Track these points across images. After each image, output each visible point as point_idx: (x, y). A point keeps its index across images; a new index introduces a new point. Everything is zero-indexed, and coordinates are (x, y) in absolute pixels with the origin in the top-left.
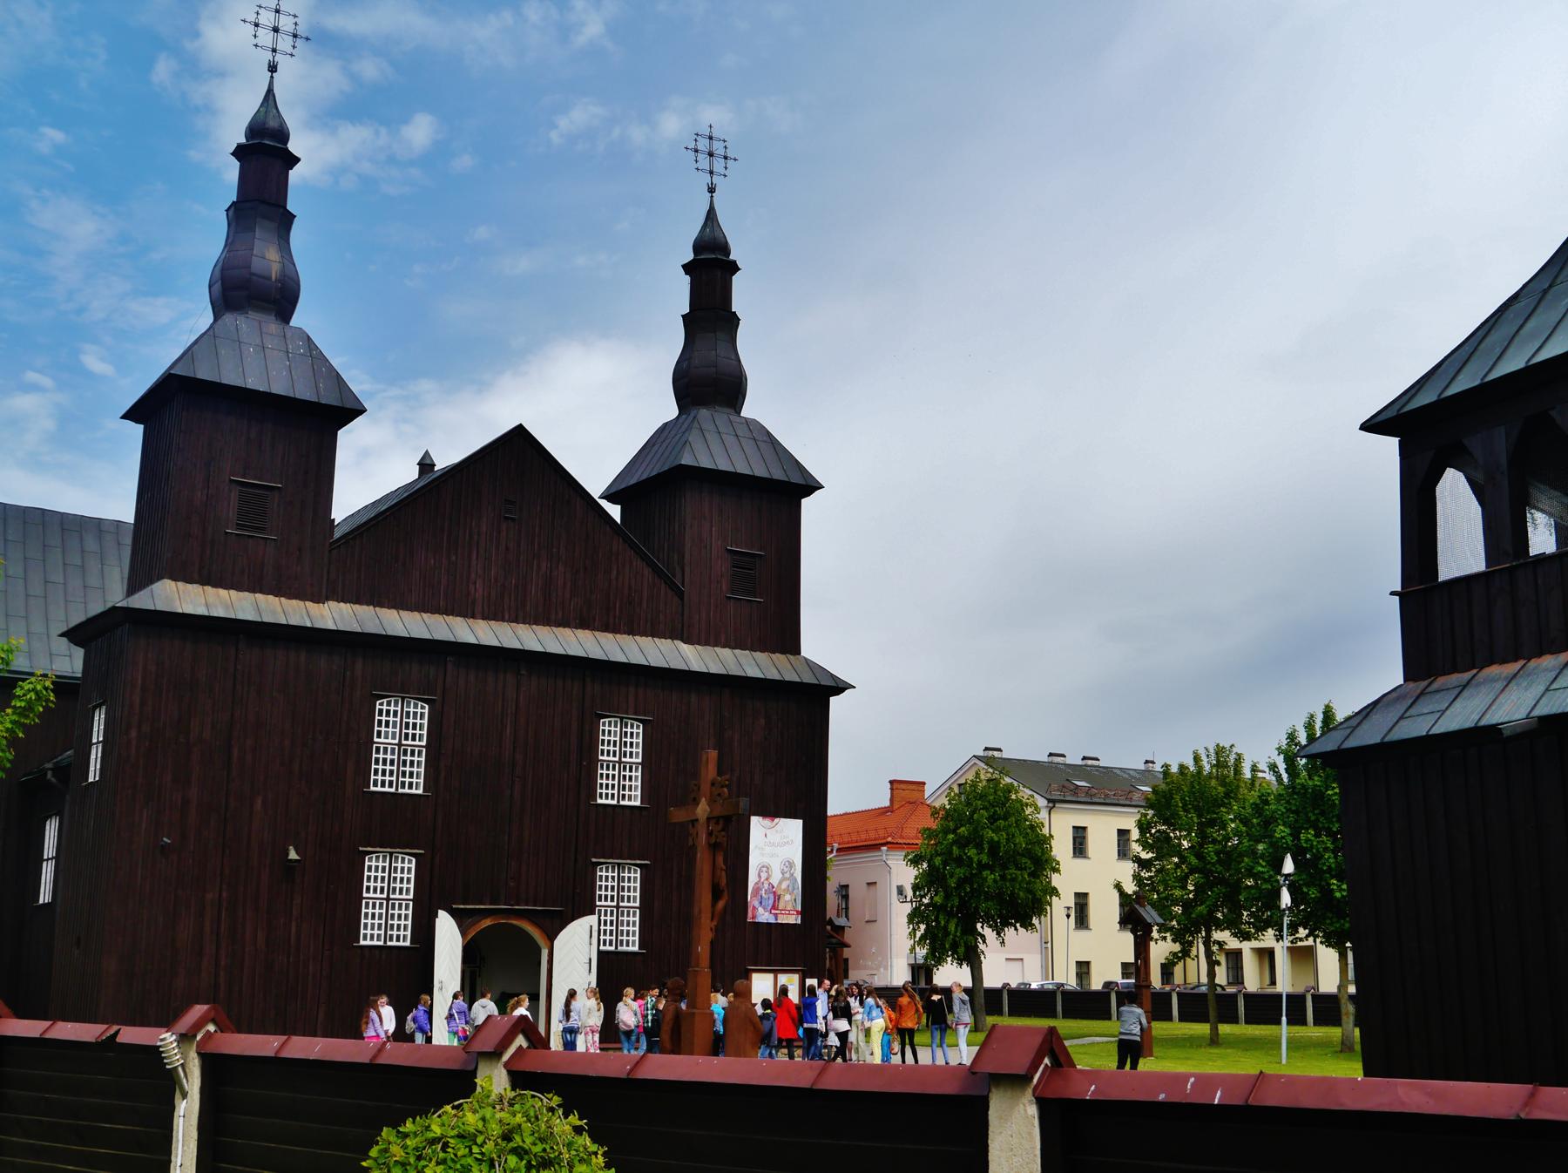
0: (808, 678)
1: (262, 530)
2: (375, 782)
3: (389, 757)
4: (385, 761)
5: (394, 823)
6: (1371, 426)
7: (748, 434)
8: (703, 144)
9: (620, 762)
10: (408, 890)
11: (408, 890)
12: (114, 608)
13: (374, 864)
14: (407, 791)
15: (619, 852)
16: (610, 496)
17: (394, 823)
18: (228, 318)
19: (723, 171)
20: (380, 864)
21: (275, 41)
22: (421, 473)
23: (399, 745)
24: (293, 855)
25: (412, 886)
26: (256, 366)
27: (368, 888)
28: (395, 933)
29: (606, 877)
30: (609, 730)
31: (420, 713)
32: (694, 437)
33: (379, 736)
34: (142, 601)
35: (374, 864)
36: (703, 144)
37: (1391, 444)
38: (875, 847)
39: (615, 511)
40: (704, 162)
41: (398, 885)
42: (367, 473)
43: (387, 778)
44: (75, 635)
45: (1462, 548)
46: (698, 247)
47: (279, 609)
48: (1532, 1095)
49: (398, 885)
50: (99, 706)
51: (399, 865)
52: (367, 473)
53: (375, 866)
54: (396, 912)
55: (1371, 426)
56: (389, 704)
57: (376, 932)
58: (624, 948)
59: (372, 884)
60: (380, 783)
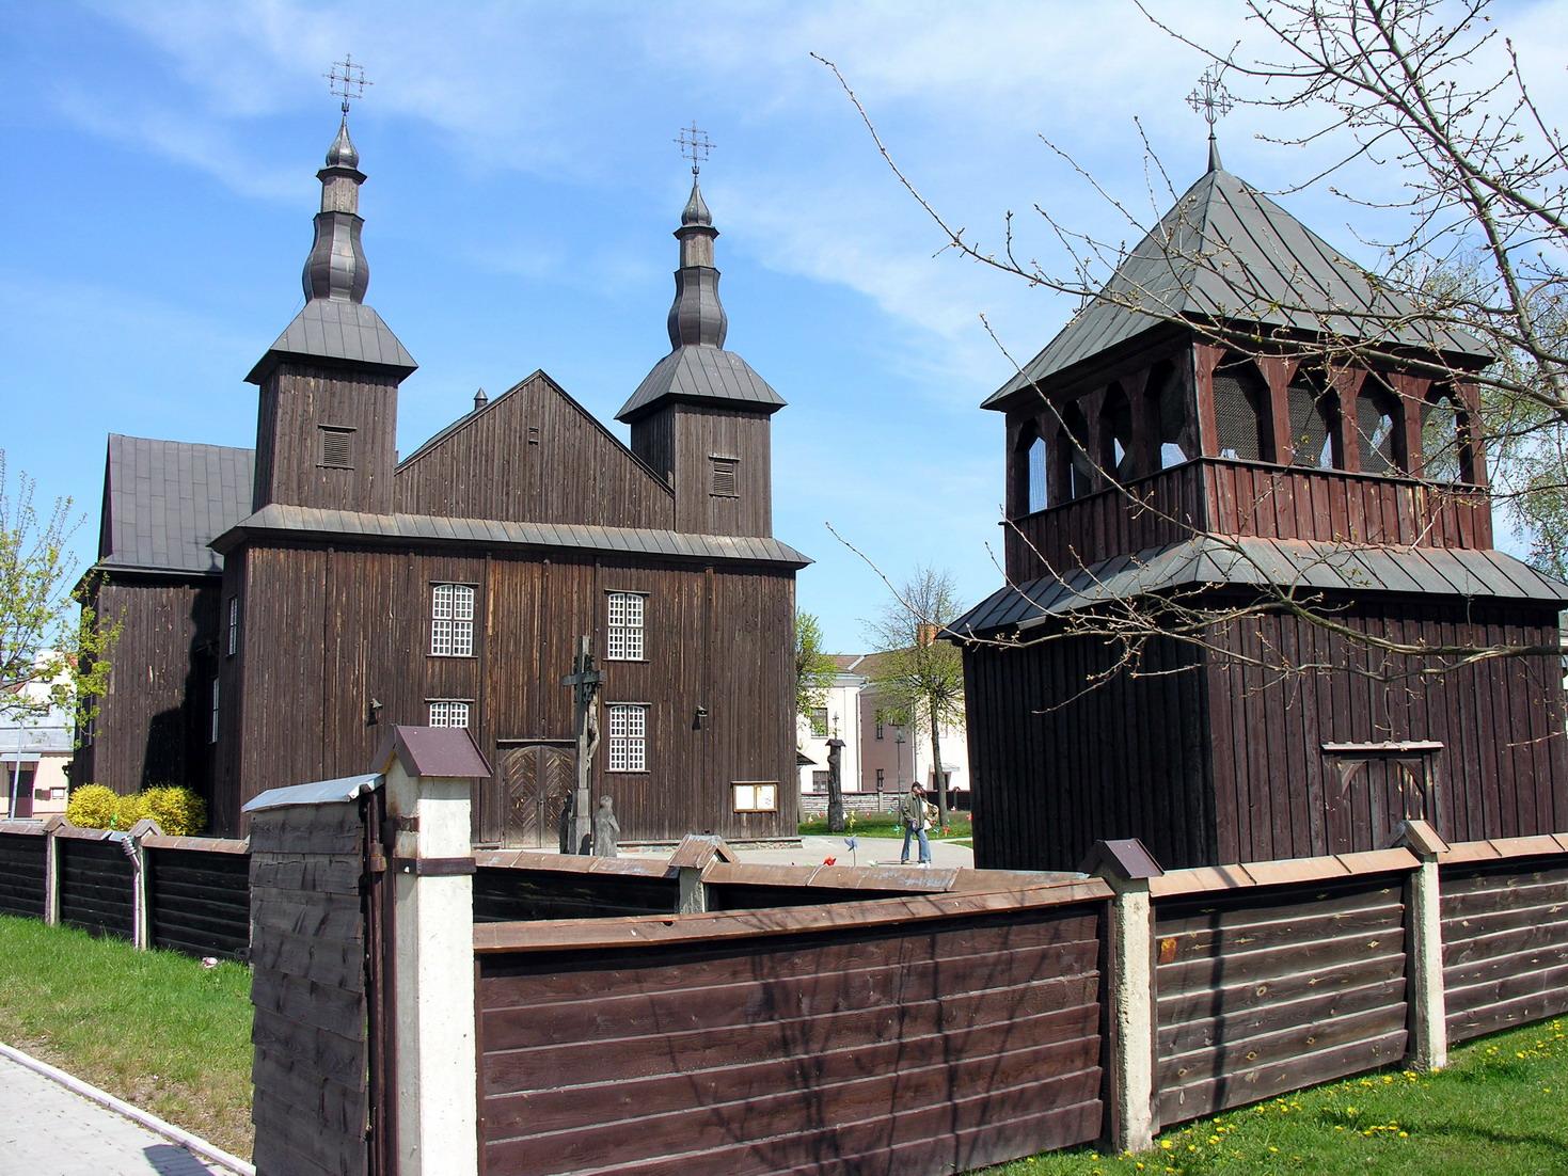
0: (777, 556)
1: (344, 461)
2: (435, 649)
3: (445, 630)
6: (988, 406)
7: (726, 364)
8: (688, 136)
9: (626, 627)
12: (236, 528)
13: (437, 710)
16: (623, 418)
18: (315, 302)
19: (705, 157)
20: (442, 710)
21: (347, 88)
22: (477, 406)
26: (335, 332)
30: (615, 604)
32: (682, 369)
33: (437, 615)
34: (257, 521)
35: (437, 710)
36: (688, 136)
37: (1000, 417)
39: (623, 432)
40: (689, 150)
42: (421, 415)
43: (444, 646)
44: (216, 545)
46: (685, 219)
47: (357, 522)
50: (233, 598)
51: (456, 711)
52: (421, 415)
55: (988, 406)
60: (440, 647)
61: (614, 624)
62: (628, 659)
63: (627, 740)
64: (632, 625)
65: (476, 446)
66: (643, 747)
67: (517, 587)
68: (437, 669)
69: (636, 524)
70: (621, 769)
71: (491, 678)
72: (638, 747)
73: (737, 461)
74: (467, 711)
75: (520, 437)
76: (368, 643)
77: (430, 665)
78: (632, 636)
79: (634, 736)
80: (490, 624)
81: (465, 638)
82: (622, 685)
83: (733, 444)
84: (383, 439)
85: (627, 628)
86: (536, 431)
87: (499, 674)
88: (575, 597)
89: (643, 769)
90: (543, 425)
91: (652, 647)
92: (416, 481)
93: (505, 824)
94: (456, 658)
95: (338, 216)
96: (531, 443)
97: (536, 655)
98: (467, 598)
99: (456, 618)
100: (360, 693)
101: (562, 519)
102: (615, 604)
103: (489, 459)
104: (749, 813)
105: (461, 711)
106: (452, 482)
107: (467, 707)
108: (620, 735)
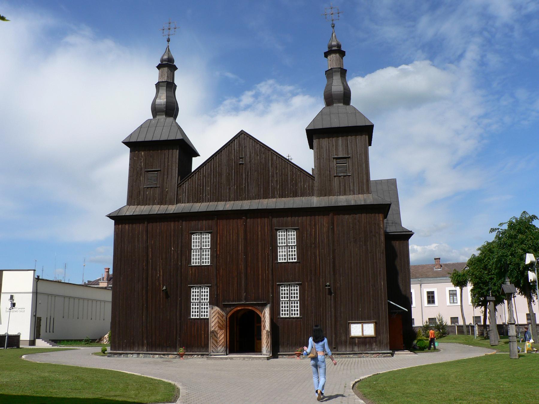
5: (201, 276)
10: (207, 299)
13: (194, 290)
14: (204, 264)
15: (289, 281)
17: (201, 276)
20: (197, 290)
23: (201, 249)
24: (164, 288)
25: (208, 297)
27: (193, 299)
28: (203, 314)
29: (284, 290)
31: (207, 238)
38: (85, 286)
41: (203, 297)
49: (203, 297)
51: (203, 290)
53: (195, 292)
54: (203, 306)
57: (196, 314)
59: (194, 297)
60: (195, 261)
64: (290, 244)
66: (298, 305)
68: (194, 272)
69: (295, 195)
70: (286, 316)
72: (296, 305)
73: (349, 158)
74: (208, 290)
78: (291, 250)
79: (293, 299)
81: (207, 257)
84: (172, 172)
85: (287, 246)
88: (260, 233)
89: (299, 316)
90: (246, 155)
95: (160, 83)
101: (258, 197)
103: (220, 174)
104: (359, 338)
105: (206, 290)
108: (286, 299)
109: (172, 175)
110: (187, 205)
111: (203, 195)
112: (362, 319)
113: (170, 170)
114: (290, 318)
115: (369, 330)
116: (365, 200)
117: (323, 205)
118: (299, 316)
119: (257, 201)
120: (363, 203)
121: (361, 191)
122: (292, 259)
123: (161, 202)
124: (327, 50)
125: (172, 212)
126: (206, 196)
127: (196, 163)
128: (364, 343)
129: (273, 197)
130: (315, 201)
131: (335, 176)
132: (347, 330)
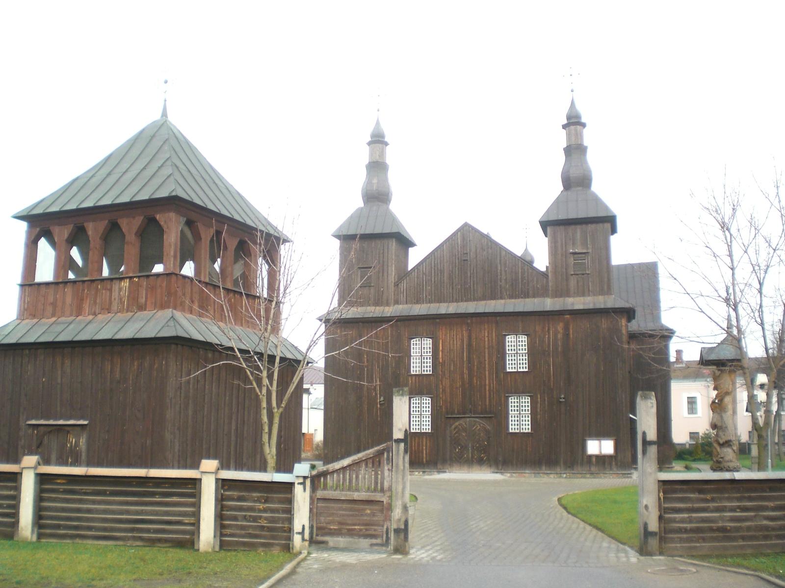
4: (512, 360)
11: (429, 411)
15: (519, 392)
30: (510, 340)
45: (45, 272)
48: (148, 471)
56: (416, 341)
58: (524, 431)
61: (510, 352)
62: (519, 370)
63: (520, 416)
65: (434, 266)
67: (454, 338)
71: (442, 384)
73: (588, 253)
75: (458, 259)
76: (380, 370)
77: (410, 379)
78: (521, 358)
80: (441, 356)
82: (517, 384)
83: (584, 243)
84: (388, 270)
86: (467, 253)
87: (447, 382)
88: (486, 339)
91: (532, 363)
92: (405, 288)
93: (451, 459)
94: (424, 374)
96: (464, 260)
97: (466, 371)
98: (428, 343)
99: (423, 355)
100: (376, 394)
101: (484, 298)
102: (510, 340)
104: (597, 456)
106: (423, 287)
107: (430, 399)
109: (388, 272)
110: (405, 306)
111: (423, 295)
112: (600, 435)
113: (385, 267)
114: (520, 433)
115: (607, 447)
116: (605, 302)
117: (557, 308)
118: (530, 431)
119: (483, 302)
120: (602, 306)
121: (602, 292)
122: (523, 367)
123: (377, 303)
124: (565, 122)
125: (388, 315)
126: (426, 296)
127: (415, 257)
128: (602, 461)
129: (501, 298)
130: (549, 304)
131: (572, 275)
132: (584, 447)
